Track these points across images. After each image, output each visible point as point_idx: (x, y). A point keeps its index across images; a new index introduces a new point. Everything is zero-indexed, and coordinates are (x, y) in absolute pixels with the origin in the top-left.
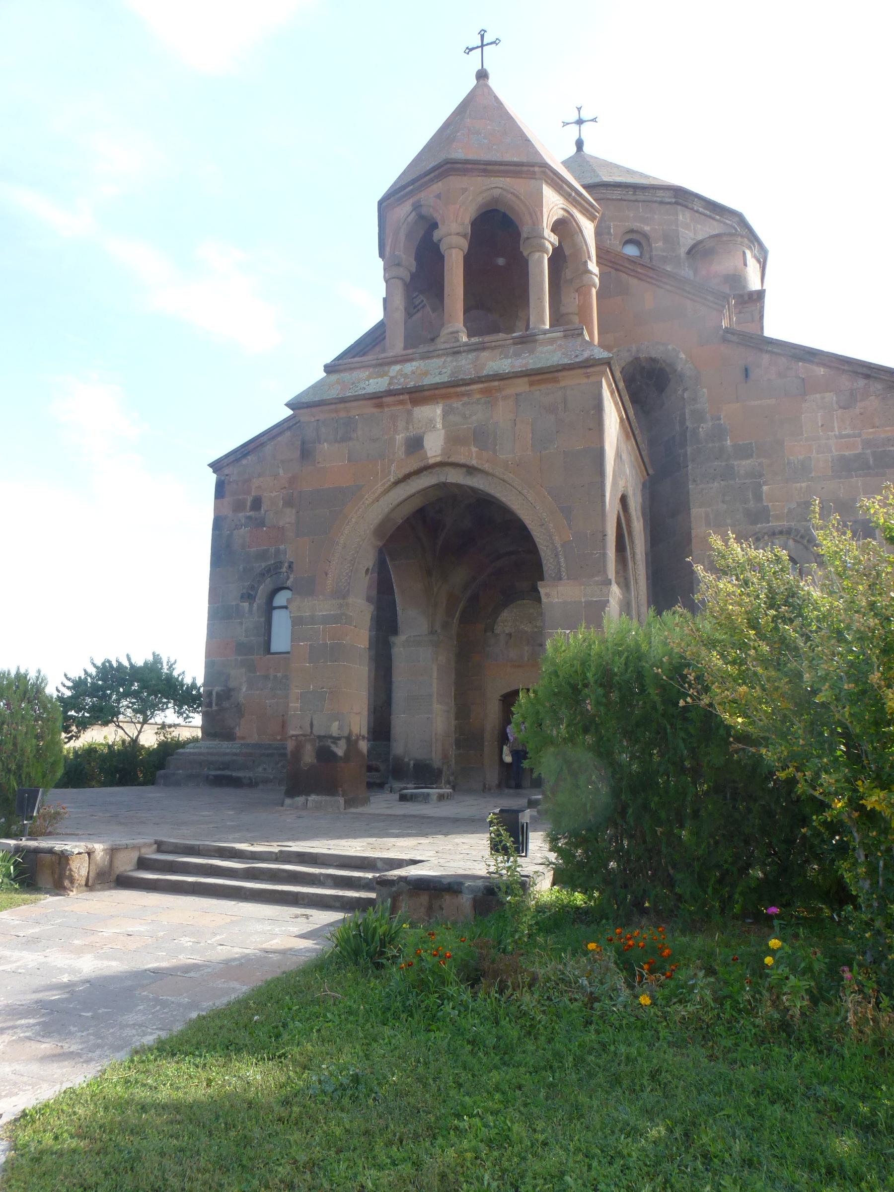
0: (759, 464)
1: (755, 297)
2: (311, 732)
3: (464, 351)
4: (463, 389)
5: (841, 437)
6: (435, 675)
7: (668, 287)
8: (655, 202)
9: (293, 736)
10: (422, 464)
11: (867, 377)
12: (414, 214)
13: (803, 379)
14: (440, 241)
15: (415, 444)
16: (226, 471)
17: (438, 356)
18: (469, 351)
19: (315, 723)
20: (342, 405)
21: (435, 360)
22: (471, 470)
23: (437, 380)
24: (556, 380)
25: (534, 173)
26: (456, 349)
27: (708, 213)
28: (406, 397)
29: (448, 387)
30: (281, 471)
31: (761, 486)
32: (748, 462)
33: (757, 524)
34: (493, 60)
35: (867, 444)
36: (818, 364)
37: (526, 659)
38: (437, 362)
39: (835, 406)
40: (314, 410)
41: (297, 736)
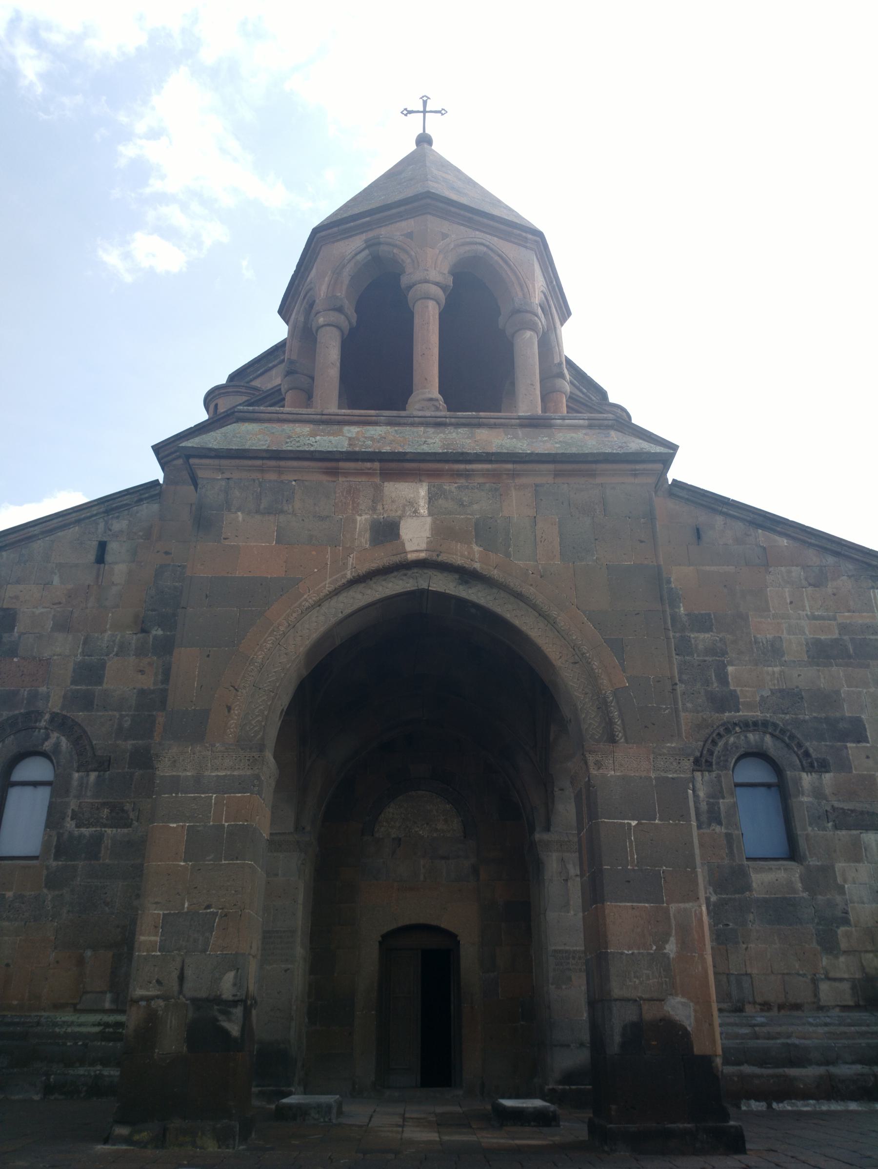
0: (721, 640)
2: (181, 992)
3: (451, 424)
4: (462, 466)
5: (815, 618)
6: (301, 898)
9: (142, 998)
10: (397, 559)
11: (837, 554)
12: (367, 252)
13: (764, 549)
14: (410, 287)
15: (387, 531)
17: (412, 424)
19: (188, 972)
22: (467, 575)
24: (592, 474)
26: (439, 420)
28: (377, 465)
29: (439, 461)
30: (56, 580)
31: (725, 666)
32: (707, 635)
33: (723, 712)
34: (435, 127)
35: (844, 628)
36: (780, 534)
37: (422, 878)
39: (804, 583)
40: (225, 462)
41: (149, 999)
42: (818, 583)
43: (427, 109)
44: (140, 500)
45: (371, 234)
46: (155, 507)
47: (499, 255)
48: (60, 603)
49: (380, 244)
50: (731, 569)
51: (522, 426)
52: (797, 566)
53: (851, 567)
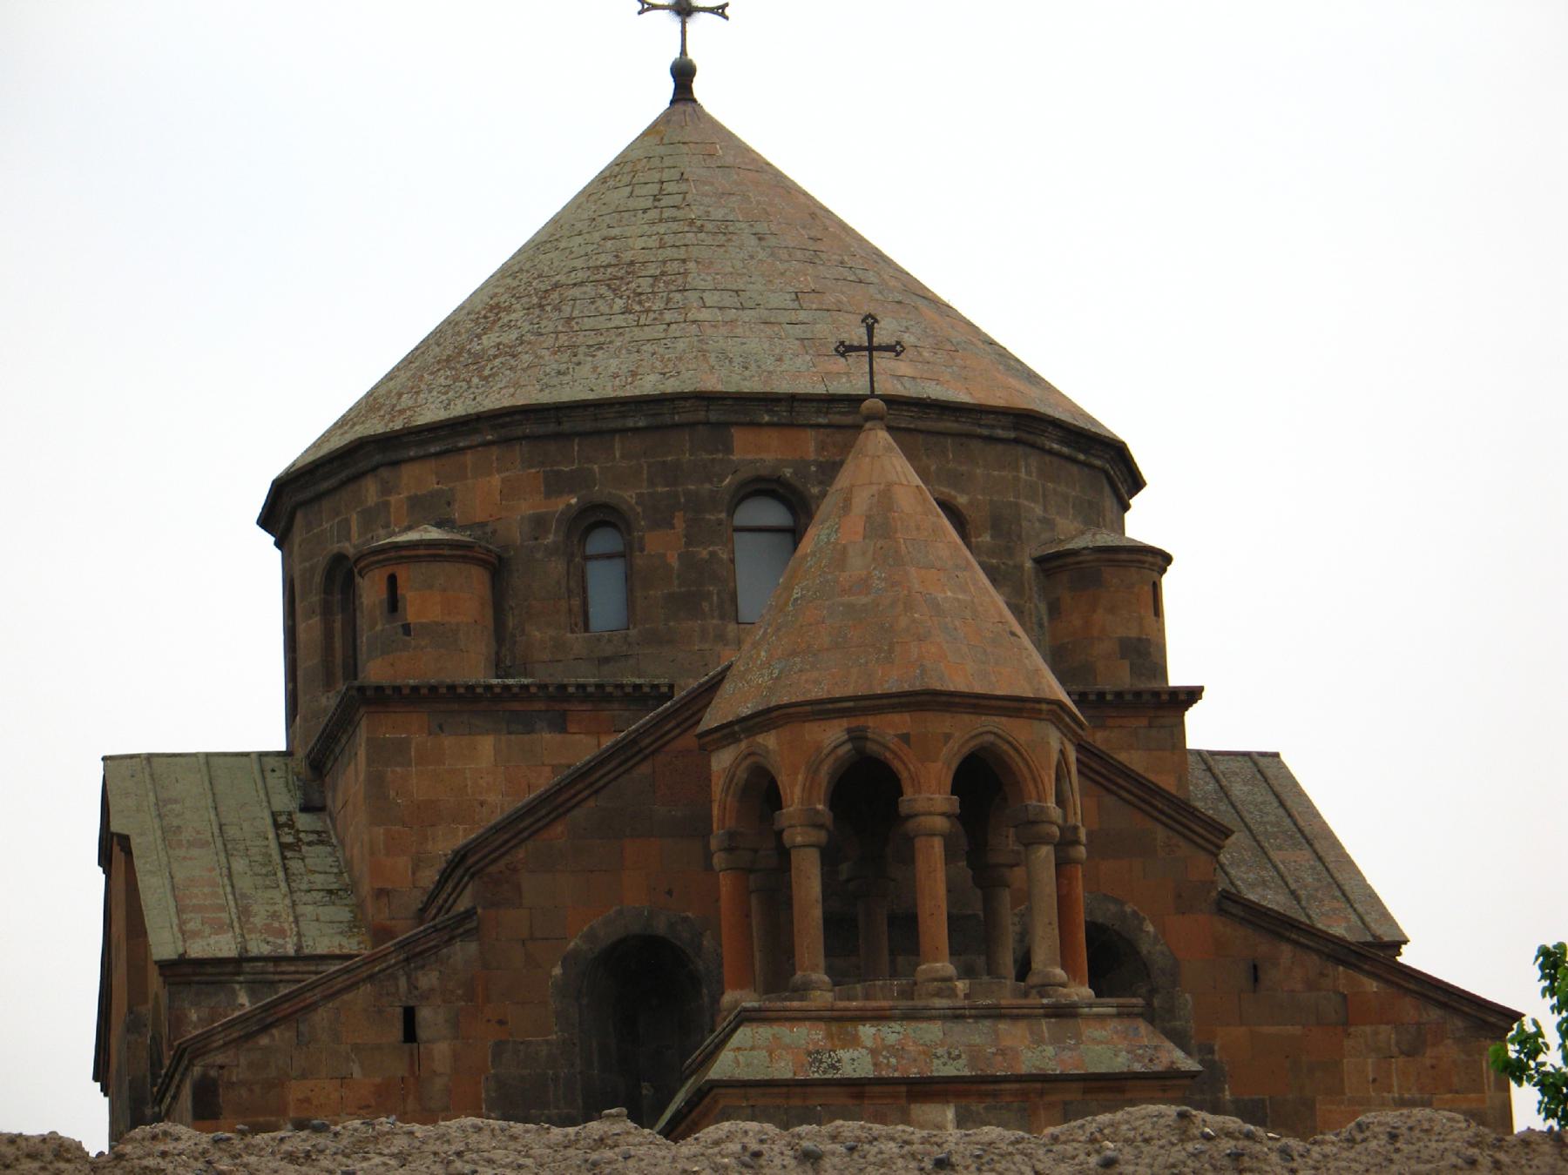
1: (1182, 697)
4: (992, 1087)
7: (1125, 794)
8: (980, 437)
11: (1444, 1006)
12: (848, 746)
13: (1345, 996)
16: (220, 1059)
17: (930, 1019)
18: (977, 1018)
20: (798, 1090)
21: (924, 1025)
23: (950, 1071)
24: (1122, 1091)
25: (1040, 711)
27: (1065, 450)
28: (903, 1089)
30: (356, 1071)
38: (933, 1031)
39: (1394, 1049)
42: (1412, 1052)
43: (876, 341)
44: (452, 939)
45: (855, 722)
46: (473, 947)
47: (1009, 743)
48: (369, 1106)
49: (867, 739)
50: (1296, 1030)
51: (1047, 1016)
52: (1387, 1023)
53: (1460, 1024)
